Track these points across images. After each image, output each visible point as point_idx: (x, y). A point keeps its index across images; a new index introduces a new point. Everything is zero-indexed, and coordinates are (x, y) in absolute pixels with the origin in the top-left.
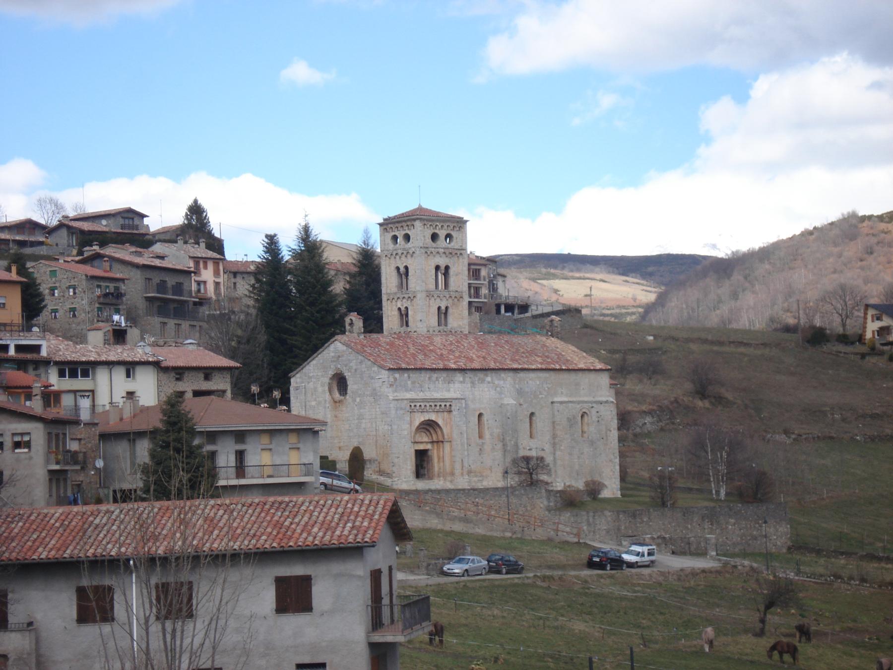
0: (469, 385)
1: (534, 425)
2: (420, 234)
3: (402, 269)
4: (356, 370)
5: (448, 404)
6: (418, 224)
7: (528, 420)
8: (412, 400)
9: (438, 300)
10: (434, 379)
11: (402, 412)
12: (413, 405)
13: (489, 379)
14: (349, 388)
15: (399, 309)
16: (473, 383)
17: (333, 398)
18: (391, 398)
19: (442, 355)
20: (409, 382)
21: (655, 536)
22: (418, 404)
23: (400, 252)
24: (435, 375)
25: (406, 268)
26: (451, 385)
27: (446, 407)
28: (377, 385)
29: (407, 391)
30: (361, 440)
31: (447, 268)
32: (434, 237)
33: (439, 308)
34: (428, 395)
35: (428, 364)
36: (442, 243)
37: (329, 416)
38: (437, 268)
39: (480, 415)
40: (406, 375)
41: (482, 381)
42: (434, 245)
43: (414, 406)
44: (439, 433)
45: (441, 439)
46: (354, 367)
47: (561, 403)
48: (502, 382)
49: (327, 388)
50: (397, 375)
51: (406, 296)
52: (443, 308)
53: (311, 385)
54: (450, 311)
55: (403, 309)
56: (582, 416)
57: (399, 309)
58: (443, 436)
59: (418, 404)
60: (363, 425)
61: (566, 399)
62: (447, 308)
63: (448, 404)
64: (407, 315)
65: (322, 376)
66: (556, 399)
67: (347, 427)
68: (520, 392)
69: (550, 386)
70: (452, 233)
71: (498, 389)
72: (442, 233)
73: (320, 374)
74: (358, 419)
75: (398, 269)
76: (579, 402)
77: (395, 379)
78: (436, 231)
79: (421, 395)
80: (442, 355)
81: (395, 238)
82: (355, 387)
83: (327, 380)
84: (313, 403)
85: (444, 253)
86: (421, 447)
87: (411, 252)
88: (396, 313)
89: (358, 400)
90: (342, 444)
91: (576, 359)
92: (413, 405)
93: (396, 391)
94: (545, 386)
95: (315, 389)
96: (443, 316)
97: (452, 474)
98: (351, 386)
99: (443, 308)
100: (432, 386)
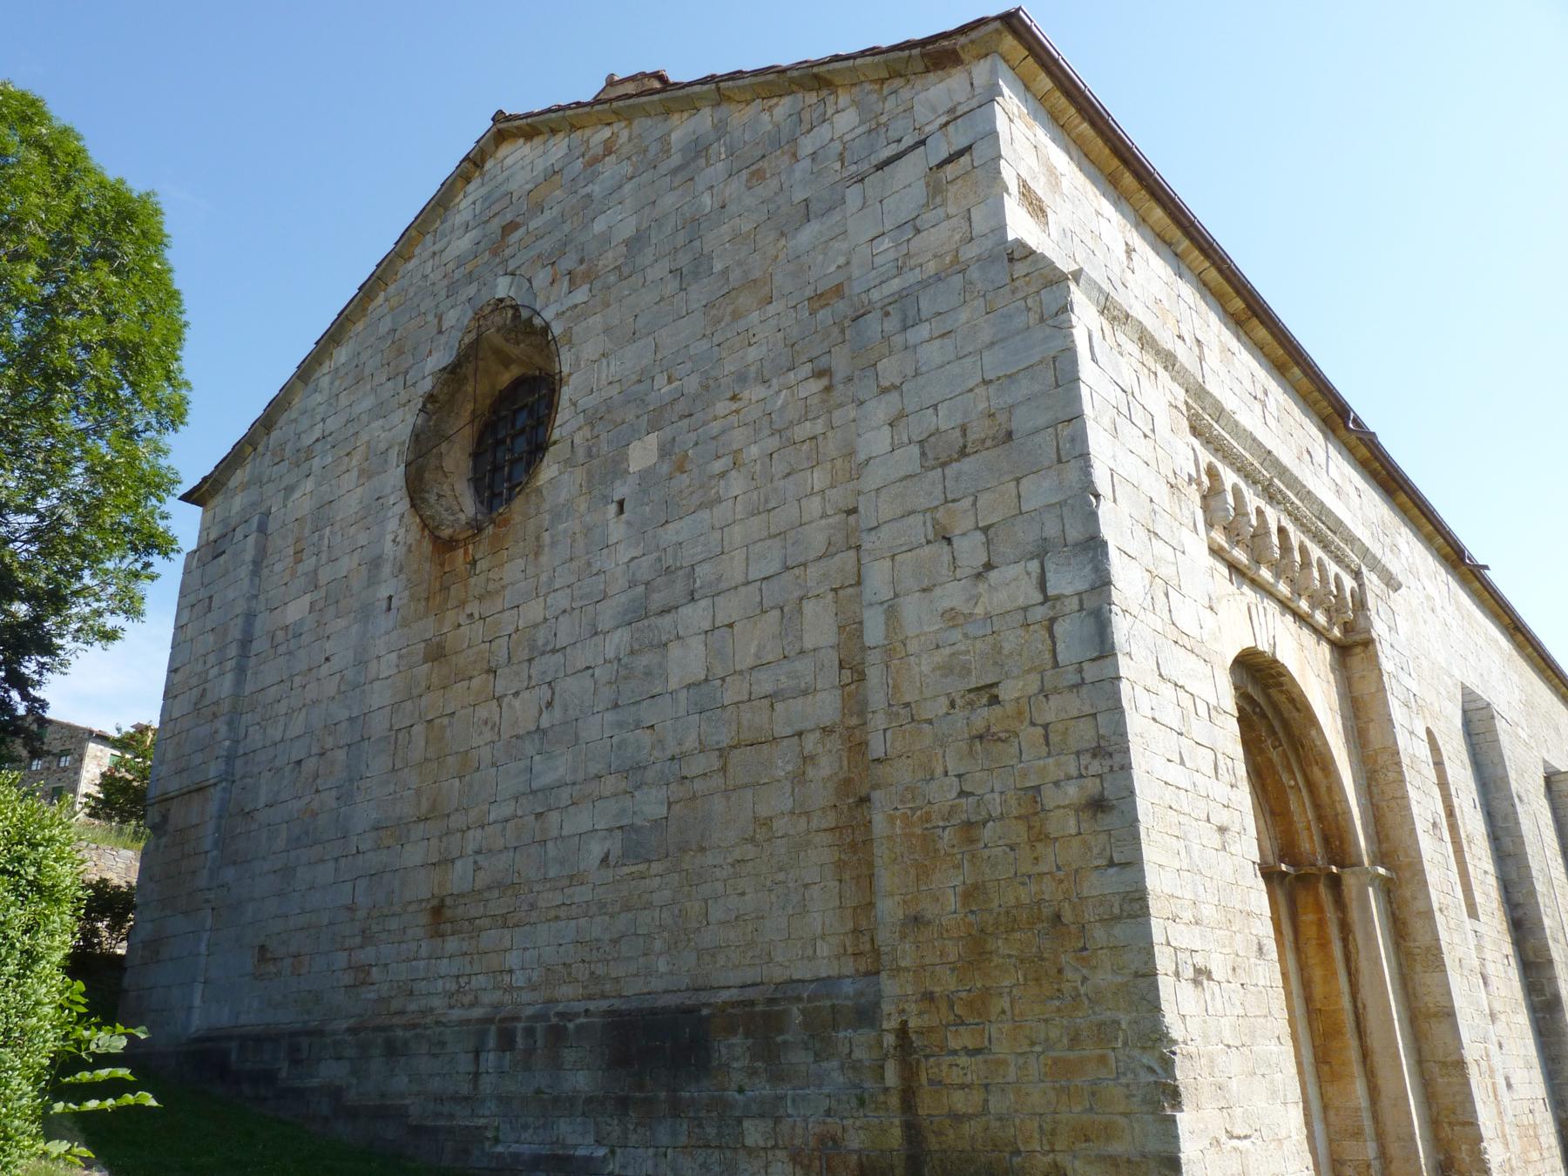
4: (635, 243)
14: (566, 393)
17: (429, 527)
30: (651, 804)
37: (386, 666)
46: (627, 230)
49: (395, 476)
53: (302, 502)
60: (688, 661)
65: (380, 411)
67: (523, 711)
73: (368, 403)
74: (636, 615)
83: (403, 423)
84: (296, 611)
89: (643, 454)
90: (459, 877)
95: (322, 514)
98: (587, 376)
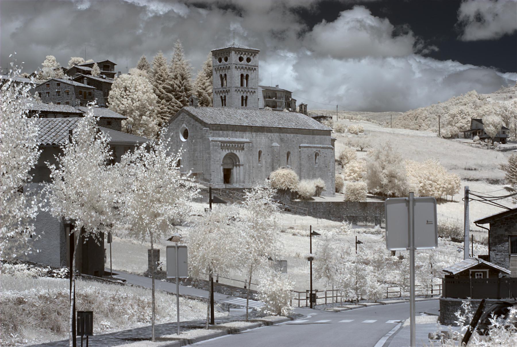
1: (289, 159)
2: (234, 58)
3: (223, 76)
4: (193, 125)
6: (233, 52)
7: (286, 155)
8: (222, 142)
9: (242, 93)
11: (216, 147)
15: (221, 97)
18: (210, 140)
19: (240, 119)
20: (221, 132)
21: (349, 215)
23: (222, 66)
25: (225, 75)
26: (244, 135)
27: (240, 146)
28: (204, 133)
29: (219, 136)
31: (247, 76)
32: (241, 59)
33: (242, 97)
34: (232, 139)
35: (232, 123)
36: (244, 62)
38: (242, 75)
39: (260, 153)
42: (240, 63)
43: (224, 145)
44: (237, 160)
45: (237, 163)
51: (225, 90)
52: (245, 97)
54: (249, 98)
55: (223, 97)
56: (316, 156)
57: (221, 97)
58: (239, 162)
60: (196, 155)
61: (307, 145)
62: (247, 97)
63: (242, 145)
64: (225, 100)
66: (301, 145)
68: (282, 140)
72: (245, 57)
75: (221, 75)
76: (314, 147)
78: (242, 56)
79: (227, 139)
80: (240, 119)
81: (220, 61)
82: (192, 134)
85: (246, 68)
86: (227, 167)
87: (228, 66)
88: (220, 99)
89: (194, 141)
91: (314, 125)
93: (213, 136)
96: (244, 101)
97: (244, 182)
99: (245, 97)
100: (233, 134)
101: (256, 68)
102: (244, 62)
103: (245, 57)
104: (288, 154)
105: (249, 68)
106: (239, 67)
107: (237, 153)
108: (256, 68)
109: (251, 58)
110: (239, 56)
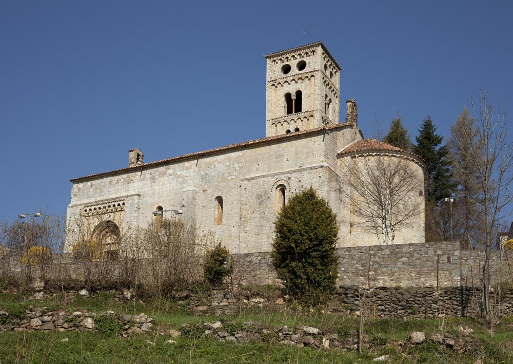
0: (149, 182)
5: (121, 203)
10: (114, 182)
12: (88, 209)
13: (171, 171)
16: (153, 179)
20: (91, 190)
22: (93, 208)
24: (115, 178)
26: (131, 185)
27: (118, 205)
29: (88, 197)
40: (89, 183)
41: (164, 174)
47: (249, 180)
48: (185, 172)
50: (81, 185)
59: (93, 208)
63: (121, 203)
68: (205, 178)
69: (240, 165)
70: (305, 59)
71: (180, 180)
72: (293, 63)
76: (273, 175)
77: (79, 189)
92: (88, 209)
94: (236, 166)
100: (111, 189)
101: (313, 74)
102: (294, 70)
103: (293, 63)
104: (220, 200)
105: (307, 77)
106: (280, 83)
107: (116, 218)
108: (313, 74)
109: (306, 59)
110: (280, 65)
